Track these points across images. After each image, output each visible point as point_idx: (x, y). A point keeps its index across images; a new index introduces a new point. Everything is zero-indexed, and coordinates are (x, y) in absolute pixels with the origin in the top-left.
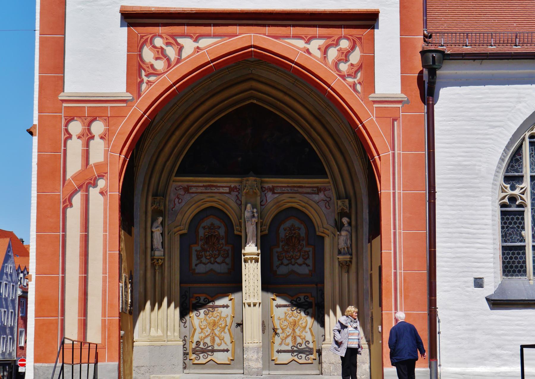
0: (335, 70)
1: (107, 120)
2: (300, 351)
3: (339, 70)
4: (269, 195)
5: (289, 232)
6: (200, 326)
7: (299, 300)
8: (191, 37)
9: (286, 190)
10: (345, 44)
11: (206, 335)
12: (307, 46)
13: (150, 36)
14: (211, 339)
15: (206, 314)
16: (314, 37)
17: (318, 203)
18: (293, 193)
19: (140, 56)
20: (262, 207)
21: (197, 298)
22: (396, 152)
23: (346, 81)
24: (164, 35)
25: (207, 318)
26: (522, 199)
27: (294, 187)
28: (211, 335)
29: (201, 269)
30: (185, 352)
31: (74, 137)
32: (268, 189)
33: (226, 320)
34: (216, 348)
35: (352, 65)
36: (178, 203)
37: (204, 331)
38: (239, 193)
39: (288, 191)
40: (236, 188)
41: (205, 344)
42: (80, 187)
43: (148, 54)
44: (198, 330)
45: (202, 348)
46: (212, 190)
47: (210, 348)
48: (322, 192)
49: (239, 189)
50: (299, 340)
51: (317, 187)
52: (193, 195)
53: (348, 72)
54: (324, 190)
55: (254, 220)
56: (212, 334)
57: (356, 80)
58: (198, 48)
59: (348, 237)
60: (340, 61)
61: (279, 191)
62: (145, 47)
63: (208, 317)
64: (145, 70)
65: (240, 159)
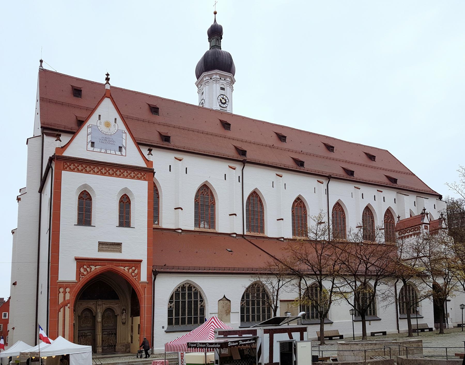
1: (70, 288)
2: (110, 346)
3: (132, 275)
8: (94, 265)
10: (133, 268)
12: (124, 268)
13: (83, 265)
15: (84, 338)
16: (126, 266)
19: (80, 270)
22: (145, 295)
24: (87, 265)
26: (173, 306)
29: (83, 325)
31: (61, 293)
42: (63, 306)
43: (82, 270)
50: (109, 343)
57: (136, 277)
58: (96, 268)
60: (132, 272)
62: (81, 268)
64: (81, 274)
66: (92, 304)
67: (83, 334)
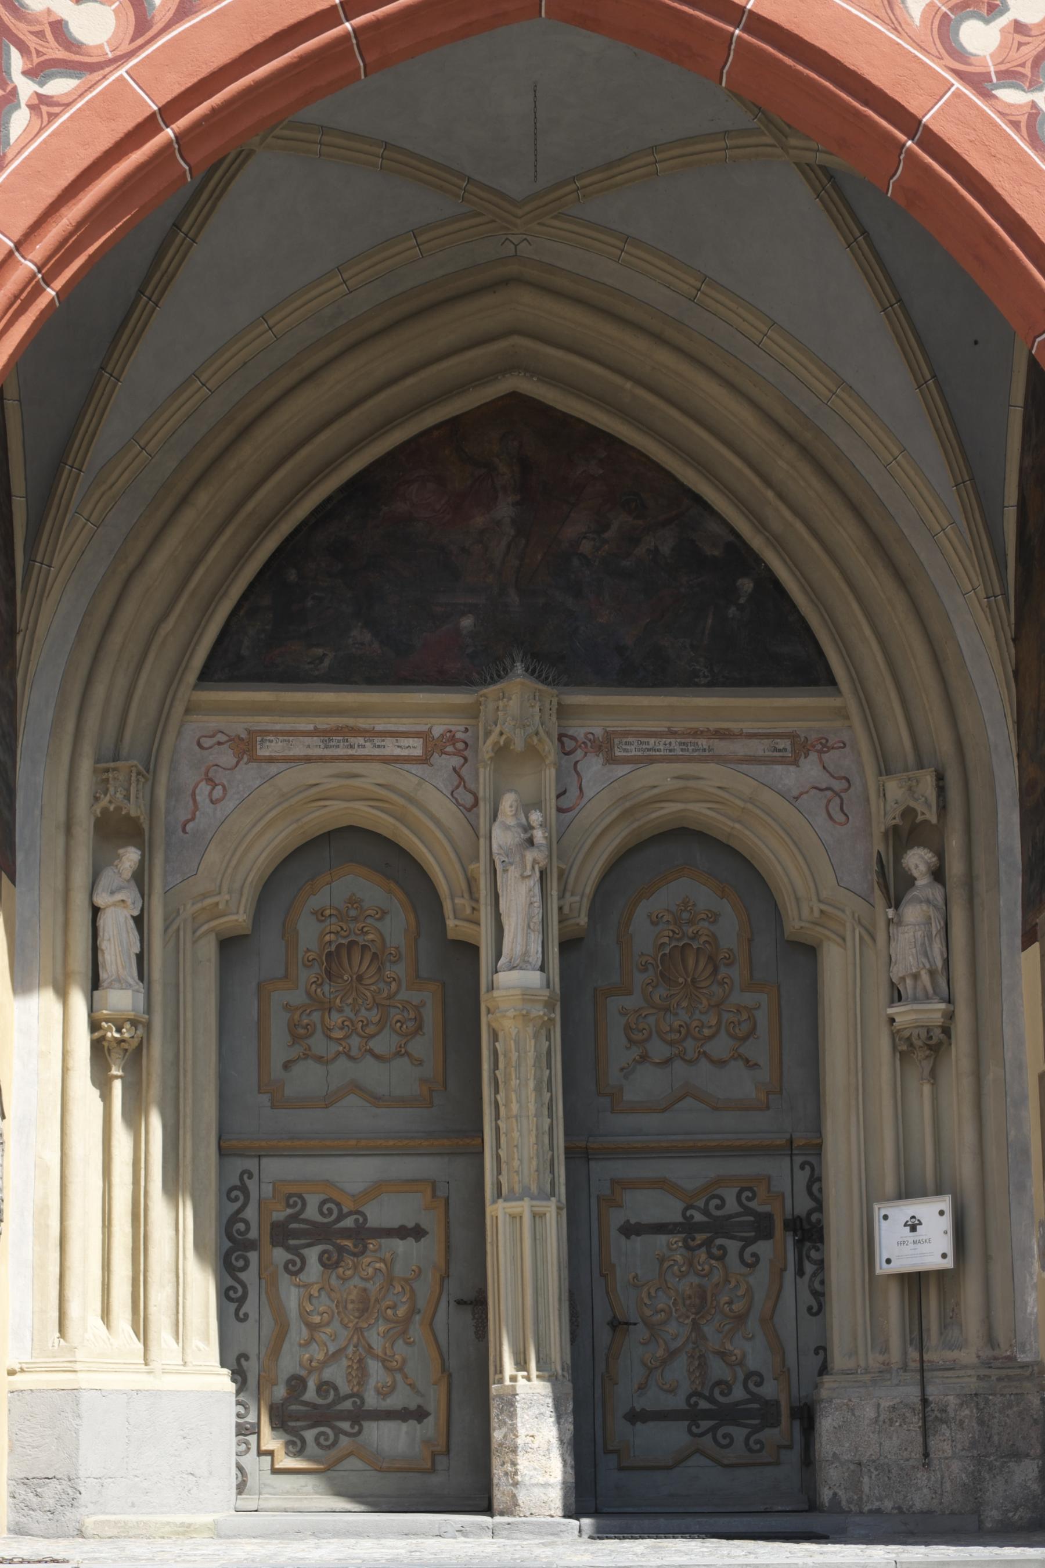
0: (942, 51)
3: (958, 53)
4: (593, 768)
5: (673, 931)
6: (304, 1315)
7: (718, 1207)
9: (662, 747)
11: (330, 1353)
14: (349, 1366)
15: (328, 1263)
17: (797, 798)
18: (690, 760)
20: (563, 816)
21: (291, 1201)
23: (993, 102)
25: (334, 1281)
27: (696, 733)
28: (351, 1349)
30: (240, 1421)
32: (589, 744)
33: (411, 1287)
34: (372, 1401)
35: (1018, 27)
36: (208, 801)
37: (322, 1336)
38: (466, 760)
39: (670, 751)
40: (453, 740)
41: (324, 1387)
44: (298, 1332)
45: (314, 1406)
46: (352, 747)
47: (347, 1405)
48: (813, 756)
49: (466, 744)
50: (718, 1369)
51: (792, 736)
52: (273, 769)
53: (1002, 63)
54: (819, 747)
55: (530, 855)
56: (356, 1346)
59: (936, 926)
61: (633, 753)
63: (338, 1277)
65: (467, 622)
66: (415, 747)
67: (311, 1213)
